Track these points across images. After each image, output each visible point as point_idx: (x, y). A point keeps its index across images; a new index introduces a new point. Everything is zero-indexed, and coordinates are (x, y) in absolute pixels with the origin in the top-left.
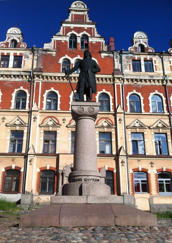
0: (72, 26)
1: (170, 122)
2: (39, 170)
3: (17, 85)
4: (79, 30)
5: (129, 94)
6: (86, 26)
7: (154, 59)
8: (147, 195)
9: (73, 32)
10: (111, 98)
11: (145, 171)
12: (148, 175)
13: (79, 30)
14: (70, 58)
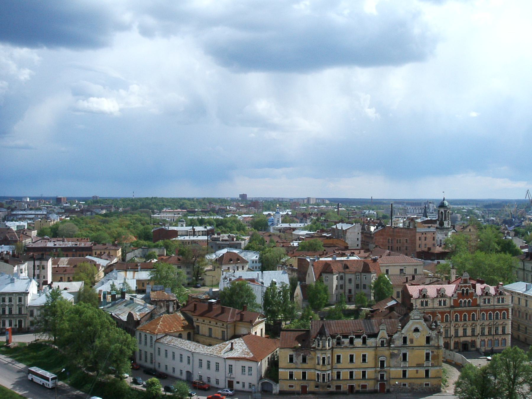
0: (463, 285)
1: (494, 323)
2: (453, 342)
3: (445, 313)
4: (465, 287)
5: (482, 313)
6: (468, 285)
7: (491, 298)
8: (484, 347)
9: (463, 288)
10: (476, 315)
11: (484, 340)
12: (485, 341)
13: (465, 287)
14: (462, 300)
